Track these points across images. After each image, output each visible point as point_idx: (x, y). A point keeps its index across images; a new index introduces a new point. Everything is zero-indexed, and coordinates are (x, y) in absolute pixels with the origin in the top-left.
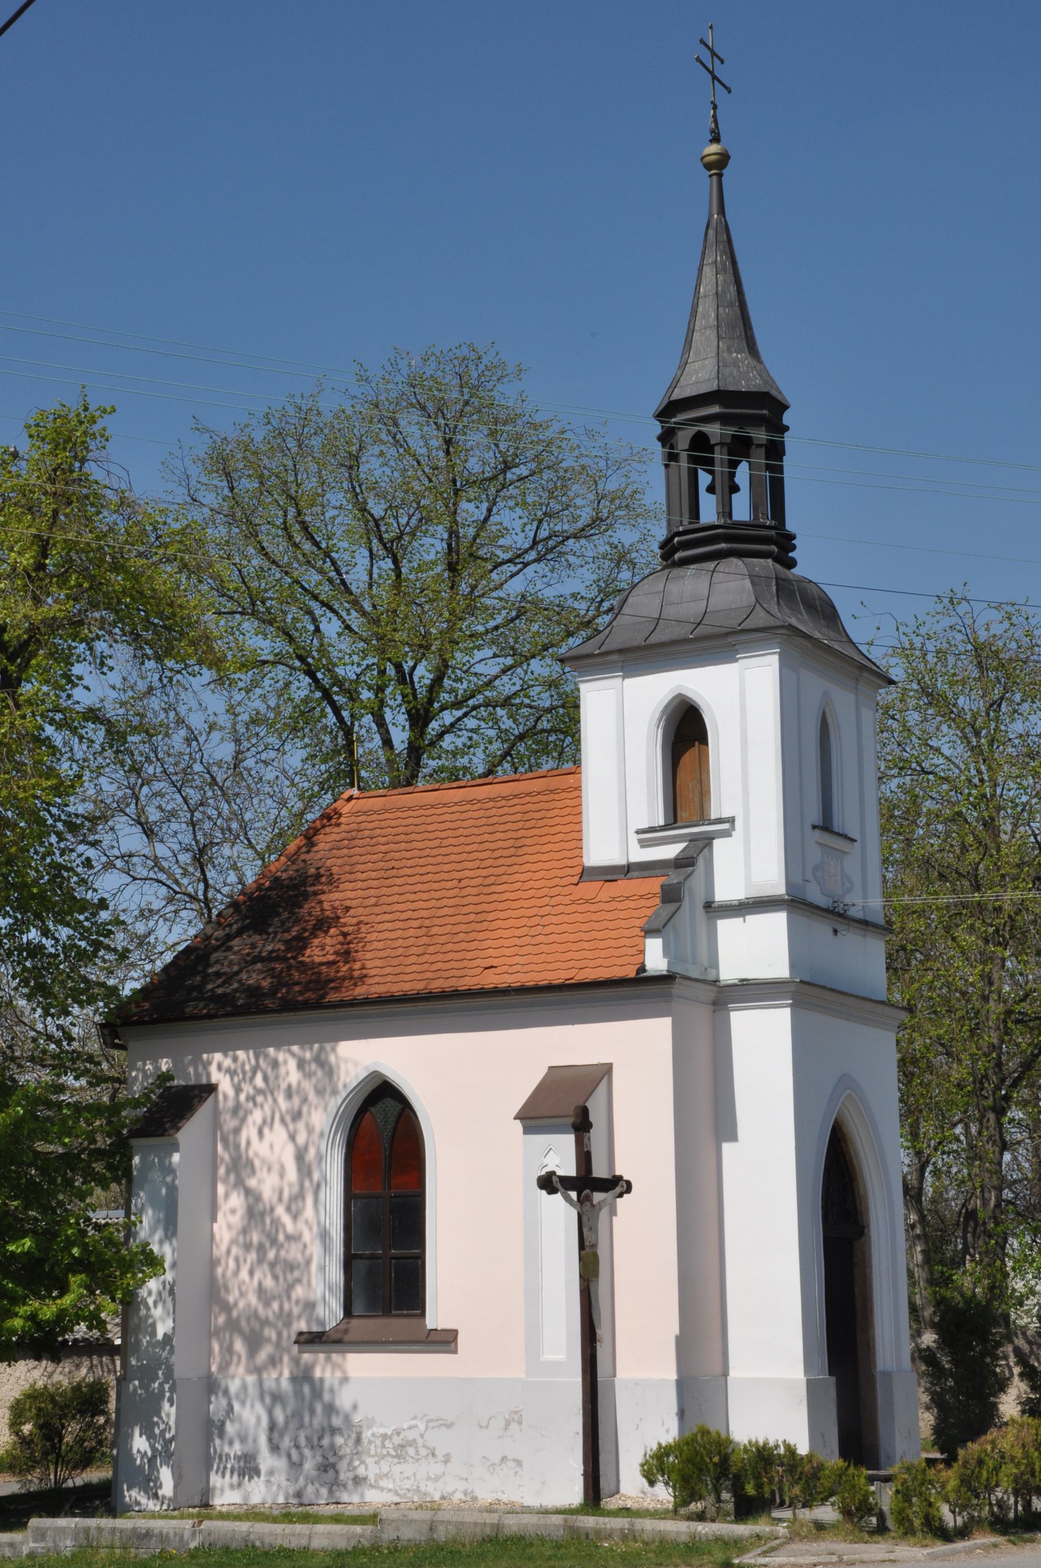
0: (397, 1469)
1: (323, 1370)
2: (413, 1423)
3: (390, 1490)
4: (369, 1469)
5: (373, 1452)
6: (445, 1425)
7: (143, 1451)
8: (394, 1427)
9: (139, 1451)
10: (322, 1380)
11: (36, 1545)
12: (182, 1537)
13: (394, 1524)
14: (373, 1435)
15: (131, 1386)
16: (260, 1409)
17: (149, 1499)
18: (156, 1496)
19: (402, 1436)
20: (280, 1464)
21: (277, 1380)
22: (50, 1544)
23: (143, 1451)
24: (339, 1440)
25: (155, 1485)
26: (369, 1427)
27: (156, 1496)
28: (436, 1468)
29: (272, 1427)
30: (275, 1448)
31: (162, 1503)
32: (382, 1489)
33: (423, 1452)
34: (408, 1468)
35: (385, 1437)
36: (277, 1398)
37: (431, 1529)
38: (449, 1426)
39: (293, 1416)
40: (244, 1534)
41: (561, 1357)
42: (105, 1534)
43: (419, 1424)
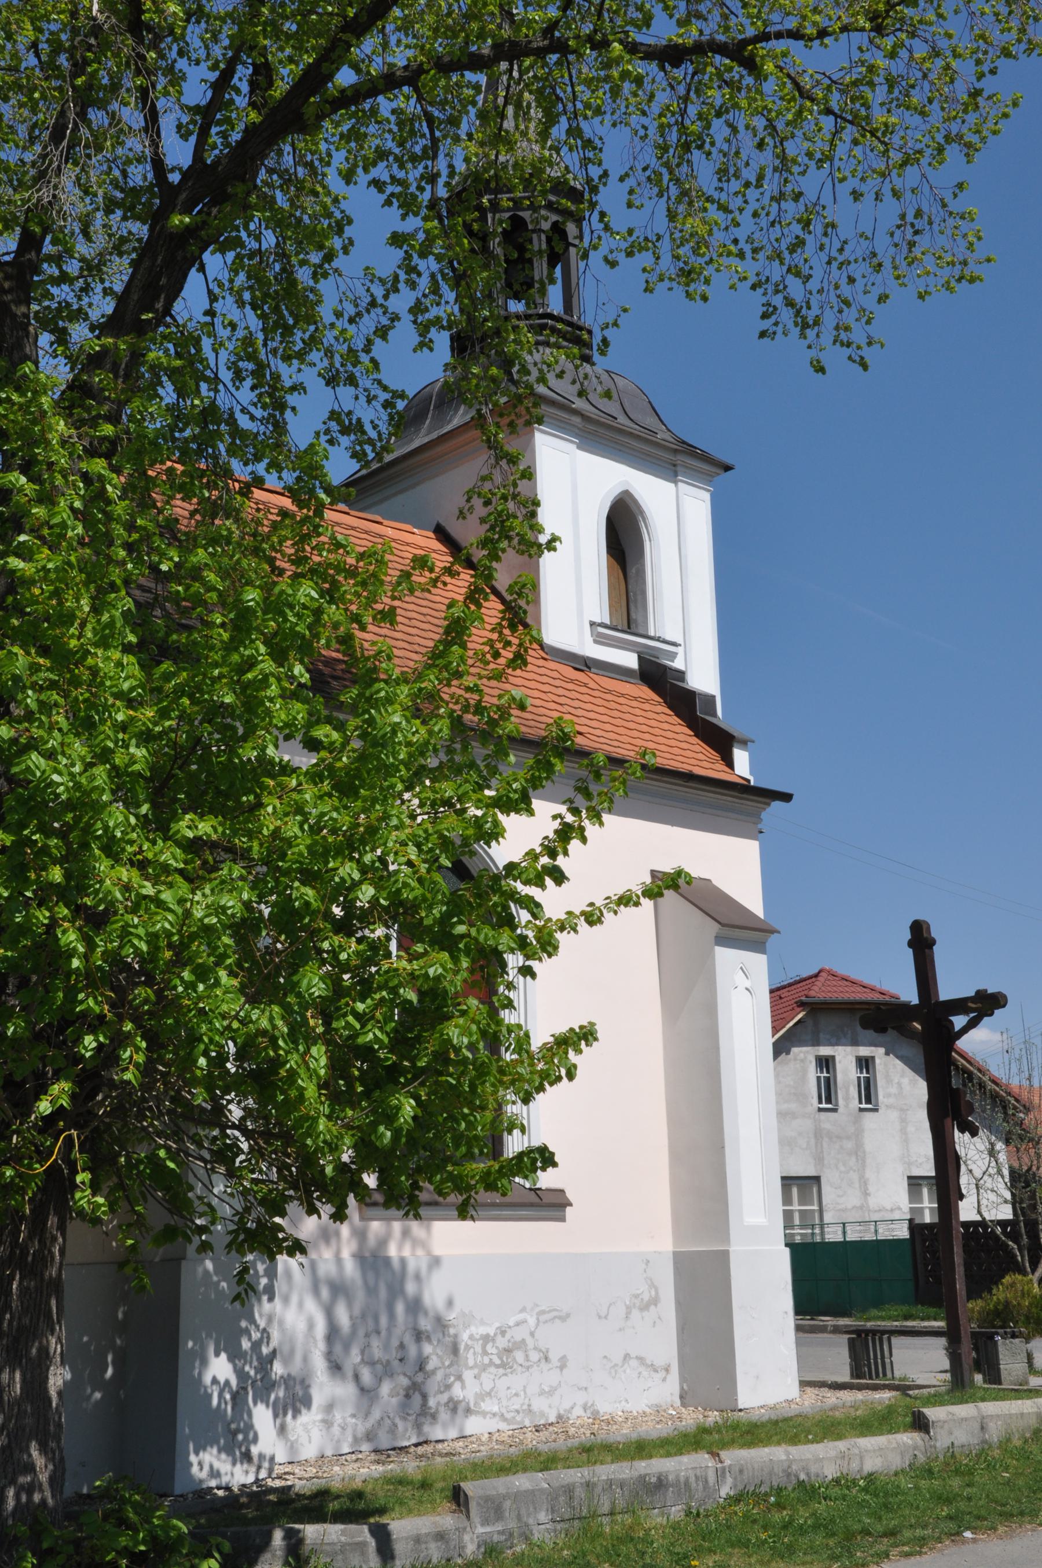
0: (503, 1383)
1: (400, 1248)
2: (521, 1316)
3: (494, 1415)
4: (465, 1391)
5: (471, 1363)
6: (560, 1318)
7: (222, 1380)
8: (497, 1325)
9: (215, 1381)
10: (403, 1261)
11: (488, 1529)
12: (706, 1481)
13: (946, 1426)
14: (471, 1337)
15: (200, 1270)
16: (311, 1306)
17: (234, 1464)
18: (247, 1457)
19: (508, 1336)
20: (346, 1390)
21: (339, 1260)
22: (512, 1524)
23: (222, 1380)
24: (428, 1349)
25: (246, 1438)
26: (466, 1326)
27: (247, 1457)
28: (550, 1377)
29: (333, 1333)
30: (336, 1367)
31: (259, 1468)
32: (484, 1414)
33: (534, 1356)
34: (516, 1381)
35: (486, 1339)
36: (338, 1289)
37: (982, 1428)
38: (564, 1318)
39: (363, 1316)
40: (786, 1465)
41: (760, 1220)
42: (580, 1493)
43: (528, 1317)
